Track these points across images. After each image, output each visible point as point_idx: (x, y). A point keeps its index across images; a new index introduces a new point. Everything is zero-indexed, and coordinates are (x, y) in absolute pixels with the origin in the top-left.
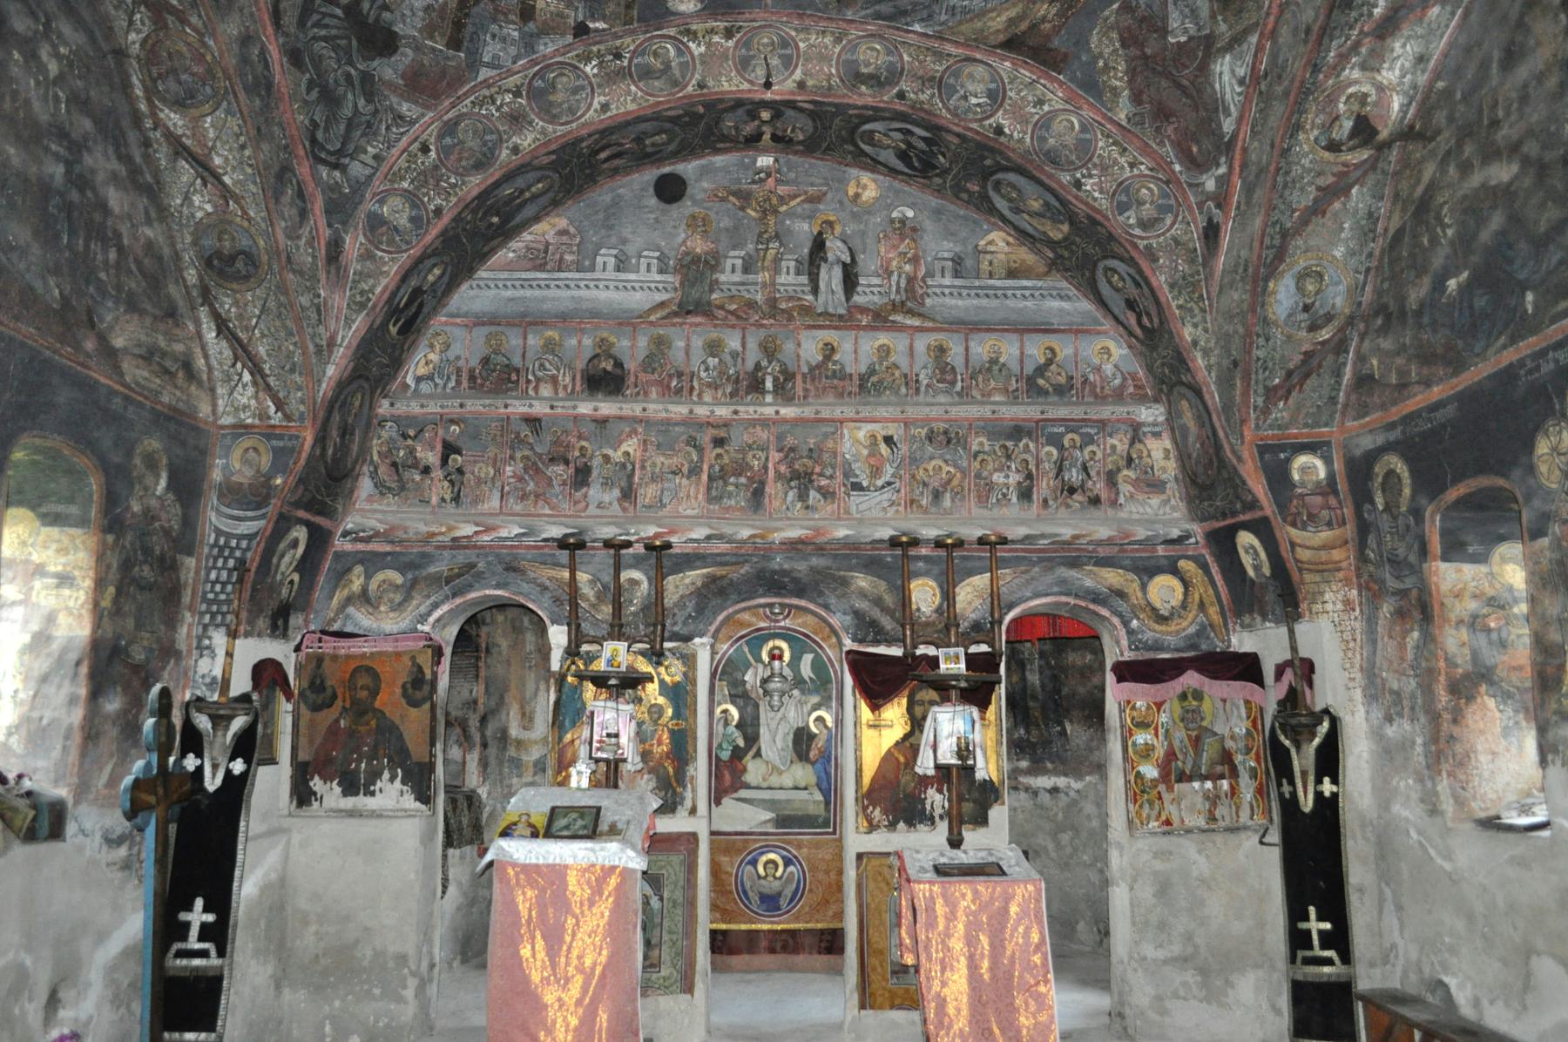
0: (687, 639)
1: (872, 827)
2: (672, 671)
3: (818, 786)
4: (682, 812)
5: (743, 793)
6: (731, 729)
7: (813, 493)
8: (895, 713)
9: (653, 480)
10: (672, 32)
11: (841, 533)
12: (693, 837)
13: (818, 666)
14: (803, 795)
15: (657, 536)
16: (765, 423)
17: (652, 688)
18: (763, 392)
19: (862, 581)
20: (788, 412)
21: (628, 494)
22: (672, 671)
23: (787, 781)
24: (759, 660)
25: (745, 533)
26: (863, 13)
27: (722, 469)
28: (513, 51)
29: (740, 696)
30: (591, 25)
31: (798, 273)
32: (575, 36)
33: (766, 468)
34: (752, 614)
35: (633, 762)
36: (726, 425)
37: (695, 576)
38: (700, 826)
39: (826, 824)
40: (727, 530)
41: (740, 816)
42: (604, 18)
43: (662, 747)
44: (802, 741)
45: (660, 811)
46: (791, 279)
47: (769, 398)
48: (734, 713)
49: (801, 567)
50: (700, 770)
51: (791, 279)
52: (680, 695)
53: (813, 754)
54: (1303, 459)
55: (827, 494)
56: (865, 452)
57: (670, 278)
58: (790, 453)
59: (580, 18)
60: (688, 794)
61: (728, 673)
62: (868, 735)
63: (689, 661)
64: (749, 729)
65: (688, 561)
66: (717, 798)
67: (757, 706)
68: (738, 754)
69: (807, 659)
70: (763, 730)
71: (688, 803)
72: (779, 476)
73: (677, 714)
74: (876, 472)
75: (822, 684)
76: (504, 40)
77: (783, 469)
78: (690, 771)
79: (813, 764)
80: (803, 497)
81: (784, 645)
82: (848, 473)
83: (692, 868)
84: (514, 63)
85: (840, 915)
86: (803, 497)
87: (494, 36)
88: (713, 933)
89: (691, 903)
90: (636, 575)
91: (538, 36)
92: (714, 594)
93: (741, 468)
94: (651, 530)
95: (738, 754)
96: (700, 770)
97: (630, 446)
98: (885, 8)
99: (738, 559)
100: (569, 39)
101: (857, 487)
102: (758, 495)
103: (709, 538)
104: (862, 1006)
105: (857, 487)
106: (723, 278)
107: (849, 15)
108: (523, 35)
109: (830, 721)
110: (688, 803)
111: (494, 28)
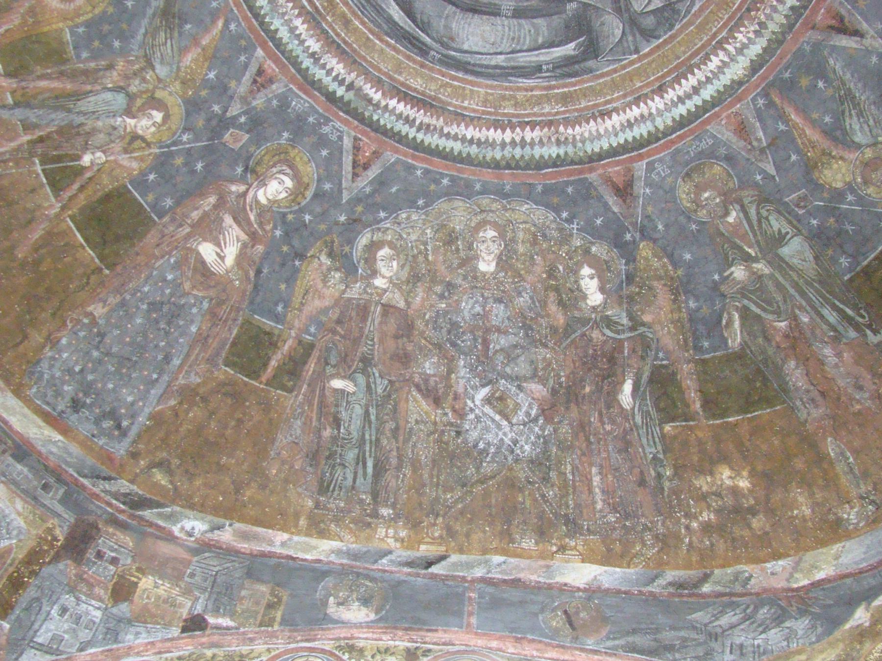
10: (328, 646)
26: (610, 643)
28: (85, 635)
30: (211, 620)
32: (184, 630)
42: (232, 615)
59: (199, 609)
76: (78, 619)
84: (81, 650)
87: (64, 610)
91: (130, 622)
98: (638, 640)
100: (175, 632)
107: (590, 643)
108: (107, 616)
111: (68, 600)
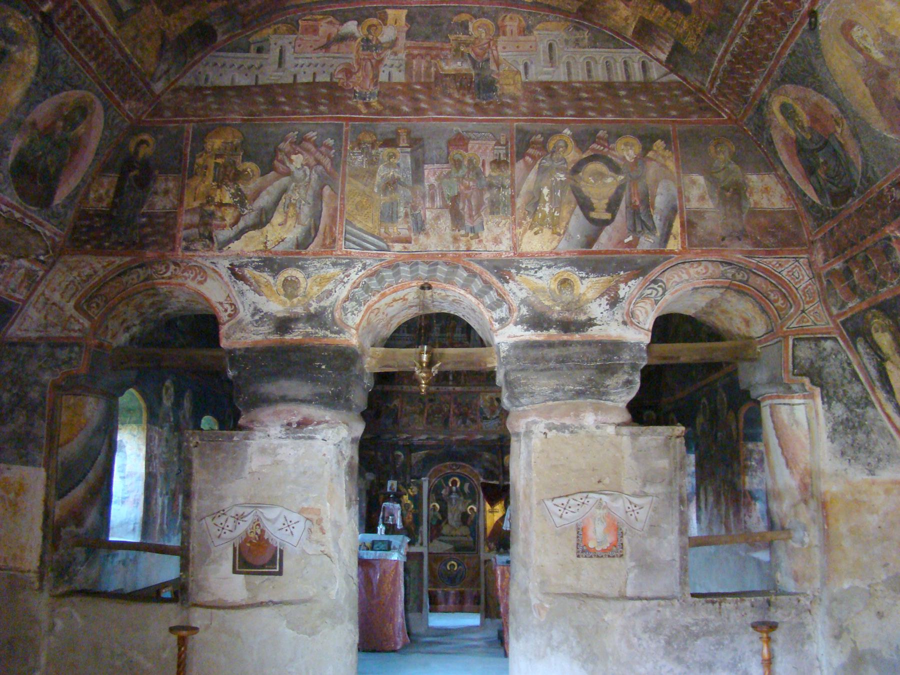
0: (419, 478)
1: (490, 550)
2: (413, 491)
3: (471, 535)
4: (417, 545)
5: (442, 538)
6: (437, 513)
7: (468, 422)
8: (499, 507)
9: (406, 415)
11: (479, 437)
12: (421, 554)
13: (471, 488)
14: (464, 539)
15: (407, 438)
16: (449, 393)
17: (406, 497)
18: (448, 380)
19: (487, 456)
20: (458, 389)
21: (396, 421)
22: (413, 491)
23: (458, 533)
24: (447, 485)
25: (441, 437)
27: (433, 411)
29: (440, 500)
31: (462, 333)
33: (449, 411)
34: (446, 467)
35: (399, 525)
36: (434, 394)
37: (422, 453)
38: (424, 550)
39: (474, 550)
40: (434, 436)
41: (440, 547)
43: (410, 518)
44: (464, 517)
45: (410, 544)
46: (459, 335)
47: (451, 383)
48: (438, 506)
49: (463, 450)
50: (424, 528)
51: (459, 335)
52: (417, 499)
53: (469, 523)
54: (647, 412)
55: (474, 421)
56: (488, 405)
57: (412, 335)
58: (459, 405)
60: (420, 538)
61: (435, 491)
62: (489, 515)
63: (420, 487)
64: (444, 512)
65: (420, 447)
66: (431, 539)
67: (446, 504)
68: (439, 523)
69: (466, 486)
70: (449, 514)
71: (419, 541)
72: (455, 414)
73: (415, 507)
74: (493, 412)
75: (472, 497)
77: (456, 411)
78: (420, 529)
79: (469, 526)
80: (464, 422)
81: (457, 479)
82: (482, 413)
83: (421, 565)
85: (478, 586)
86: (464, 422)
88: (430, 593)
89: (421, 578)
90: (399, 453)
92: (428, 461)
93: (440, 411)
94: (405, 436)
95: (439, 523)
96: (424, 528)
97: (396, 402)
99: (438, 447)
101: (486, 418)
102: (446, 422)
103: (427, 439)
104: (486, 617)
105: (486, 418)
106: (432, 335)
109: (475, 509)
110: (419, 541)
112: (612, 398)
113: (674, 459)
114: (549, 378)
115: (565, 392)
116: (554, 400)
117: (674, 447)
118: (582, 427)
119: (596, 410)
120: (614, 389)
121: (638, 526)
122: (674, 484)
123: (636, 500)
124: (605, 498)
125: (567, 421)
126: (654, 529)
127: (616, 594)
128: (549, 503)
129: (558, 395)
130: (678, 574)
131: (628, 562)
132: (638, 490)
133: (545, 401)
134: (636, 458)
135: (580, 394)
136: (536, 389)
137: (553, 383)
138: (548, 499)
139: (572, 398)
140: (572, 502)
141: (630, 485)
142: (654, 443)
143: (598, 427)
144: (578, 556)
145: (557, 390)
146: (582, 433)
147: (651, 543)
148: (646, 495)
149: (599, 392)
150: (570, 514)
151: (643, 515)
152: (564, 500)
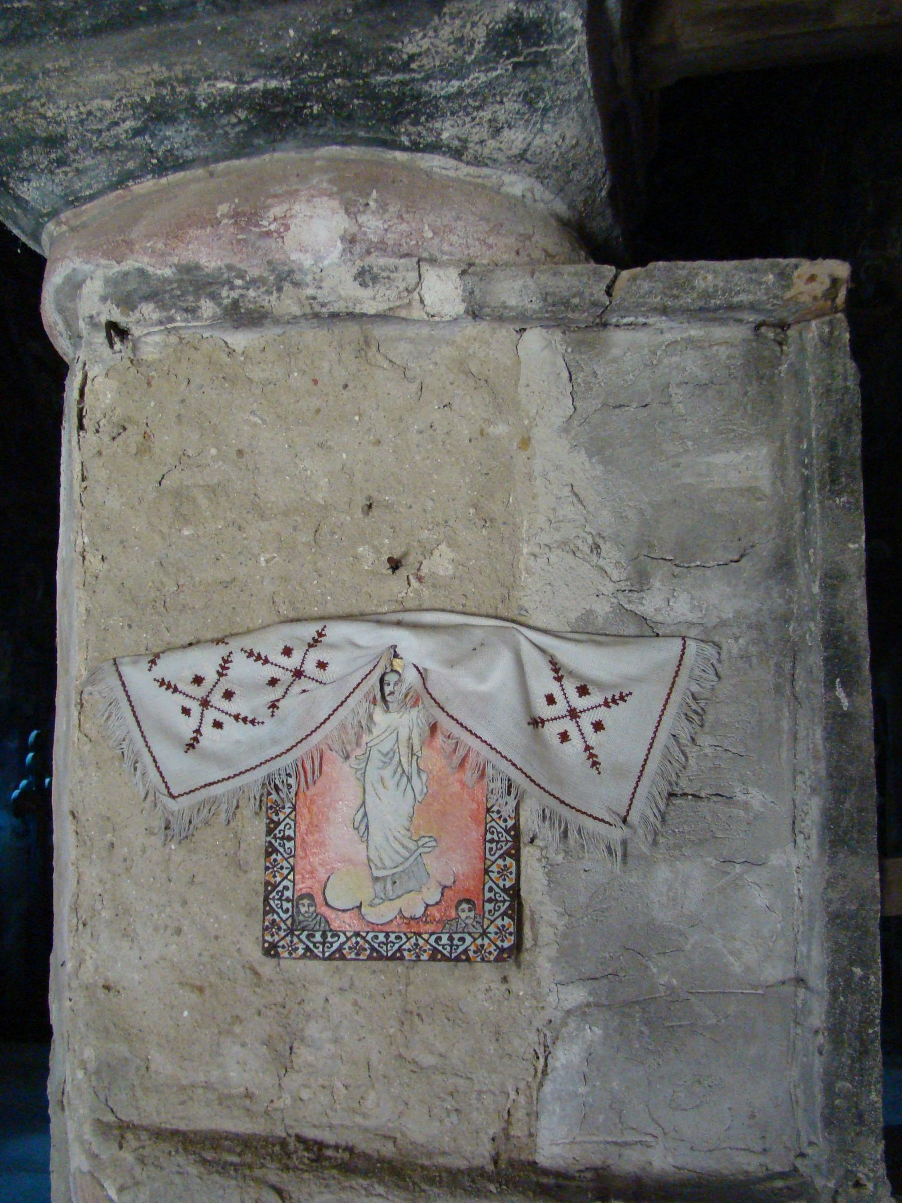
112: (448, 131)
113: (800, 434)
114: (122, 62)
115: (206, 117)
116: (161, 170)
117: (797, 375)
118: (285, 277)
119: (352, 191)
120: (448, 76)
121: (604, 795)
122: (802, 570)
123: (584, 659)
124: (413, 647)
125: (209, 256)
126: (680, 804)
127: (477, 1152)
128: (139, 678)
129: (178, 136)
130: (818, 1063)
131: (550, 986)
132: (603, 608)
133: (123, 180)
134: (598, 448)
135: (275, 119)
136: (63, 112)
137: (142, 79)
138: (136, 657)
139: (242, 148)
140: (241, 667)
141: (559, 584)
142: (692, 365)
143: (365, 277)
144: (271, 951)
145: (158, 114)
146: (287, 303)
147: (675, 885)
148: (648, 630)
149: (372, 95)
150: (234, 731)
151: (627, 736)
152: (206, 661)
